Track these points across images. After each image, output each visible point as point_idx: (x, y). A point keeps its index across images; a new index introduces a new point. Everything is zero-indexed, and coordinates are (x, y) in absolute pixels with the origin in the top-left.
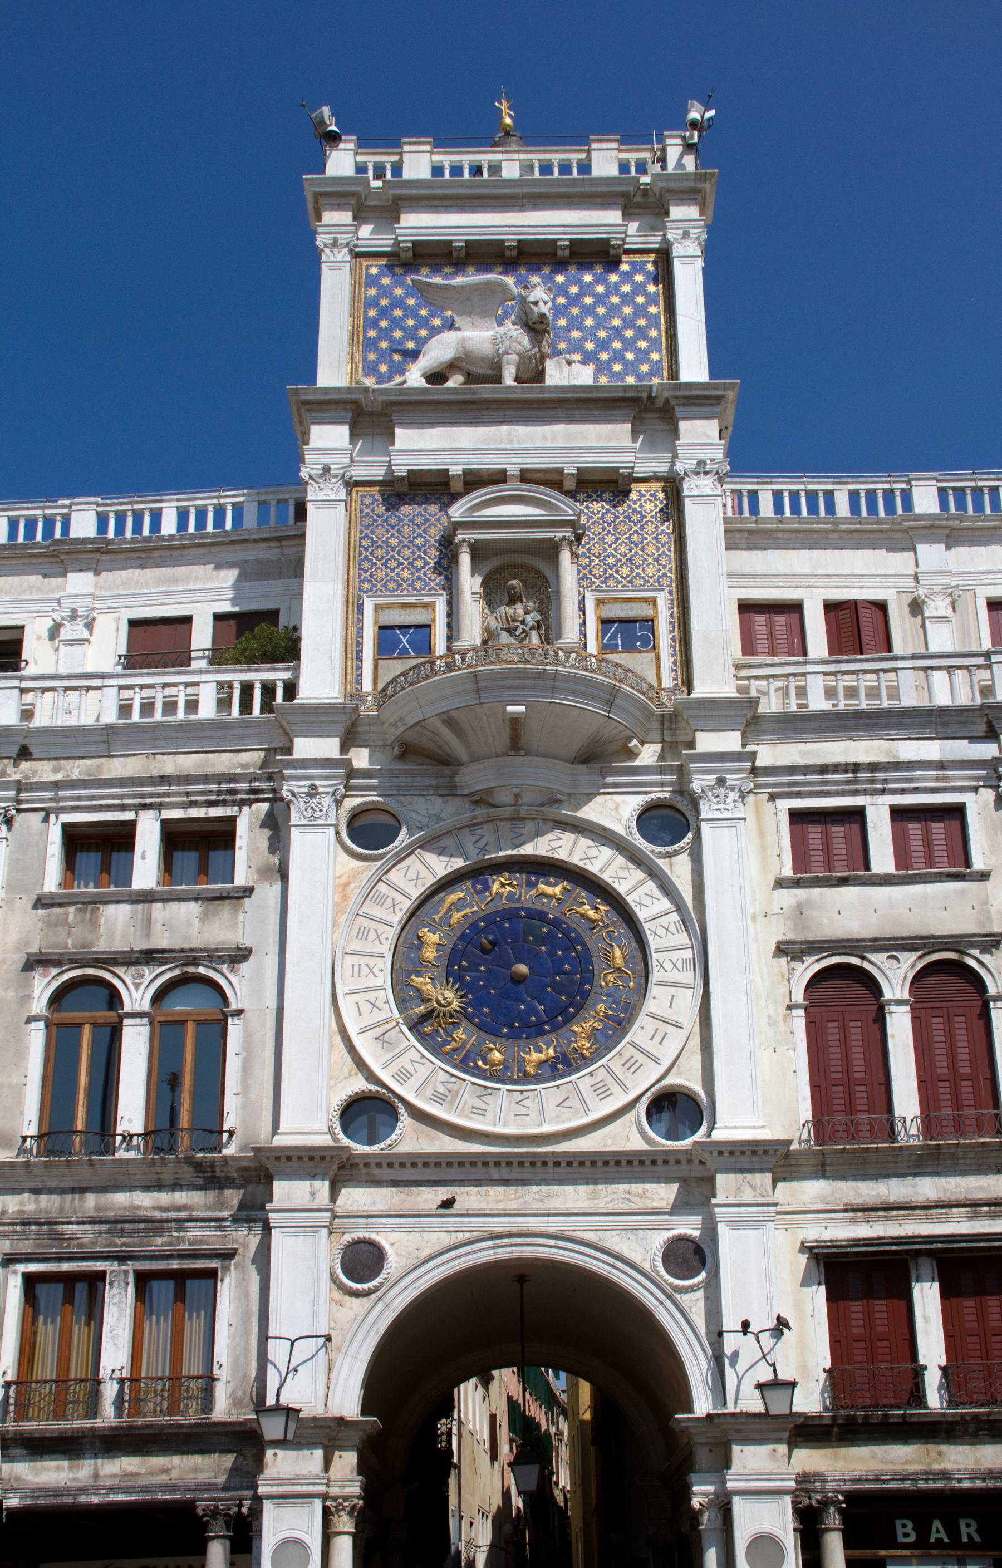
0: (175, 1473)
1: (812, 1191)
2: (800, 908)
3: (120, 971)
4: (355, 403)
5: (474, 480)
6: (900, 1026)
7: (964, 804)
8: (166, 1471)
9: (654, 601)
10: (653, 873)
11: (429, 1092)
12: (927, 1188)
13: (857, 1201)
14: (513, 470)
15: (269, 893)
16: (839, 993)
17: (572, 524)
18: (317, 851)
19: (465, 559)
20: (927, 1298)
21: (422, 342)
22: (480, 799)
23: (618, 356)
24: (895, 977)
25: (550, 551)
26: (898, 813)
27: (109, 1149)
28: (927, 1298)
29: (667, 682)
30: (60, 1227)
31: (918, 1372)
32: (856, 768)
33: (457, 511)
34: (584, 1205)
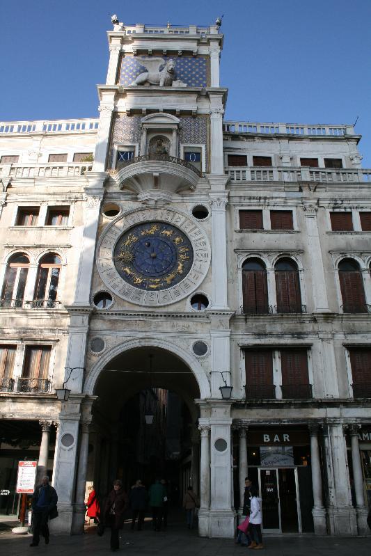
0: (34, 411)
2: (242, 240)
3: (31, 250)
4: (116, 90)
5: (149, 111)
7: (292, 211)
8: (31, 410)
9: (201, 148)
11: (122, 292)
12: (278, 328)
13: (256, 331)
14: (161, 109)
16: (253, 266)
17: (178, 125)
19: (145, 133)
20: (277, 364)
25: (170, 131)
27: (21, 306)
28: (277, 364)
29: (204, 170)
30: (5, 330)
32: (260, 198)
33: (143, 120)
34: (169, 330)
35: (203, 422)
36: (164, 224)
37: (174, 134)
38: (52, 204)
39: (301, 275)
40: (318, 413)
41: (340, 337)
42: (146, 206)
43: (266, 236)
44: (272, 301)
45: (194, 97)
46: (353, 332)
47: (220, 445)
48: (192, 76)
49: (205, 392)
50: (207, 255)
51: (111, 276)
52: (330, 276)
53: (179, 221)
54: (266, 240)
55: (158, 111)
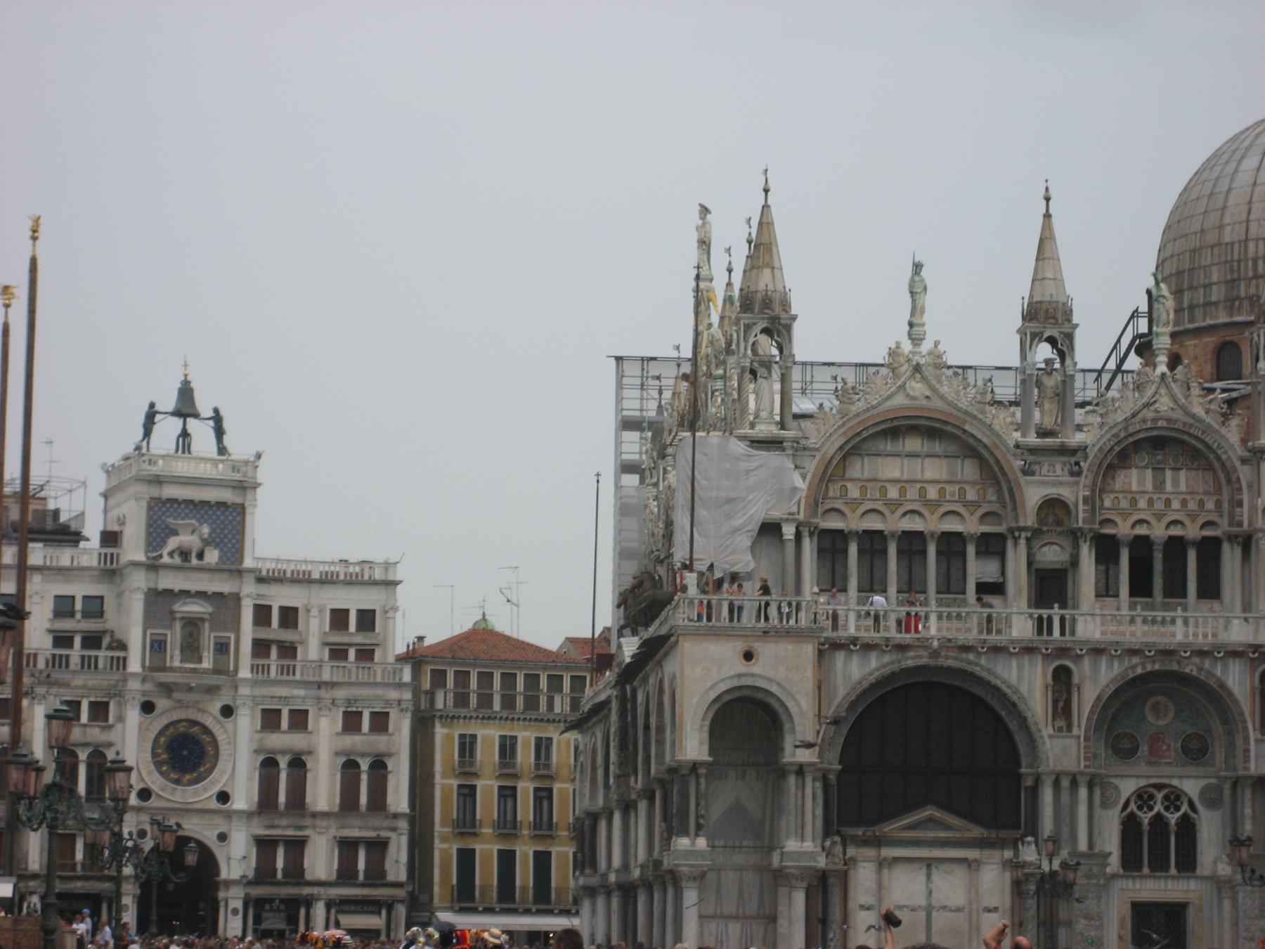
1: (256, 821)
2: (261, 739)
6: (283, 776)
10: (223, 727)
12: (284, 822)
15: (119, 726)
18: (133, 715)
20: (280, 853)
21: (168, 536)
22: (179, 701)
23: (226, 545)
24: (283, 763)
26: (291, 711)
28: (280, 853)
29: (231, 668)
31: (276, 870)
35: (221, 895)
36: (194, 723)
37: (207, 625)
38: (92, 699)
39: (309, 775)
40: (306, 891)
41: (333, 831)
42: (181, 704)
43: (283, 736)
44: (282, 798)
45: (226, 575)
46: (343, 827)
47: (235, 911)
48: (226, 536)
49: (224, 875)
50: (230, 755)
51: (150, 773)
52: (333, 775)
53: (208, 722)
54: (283, 740)
55: (186, 594)
